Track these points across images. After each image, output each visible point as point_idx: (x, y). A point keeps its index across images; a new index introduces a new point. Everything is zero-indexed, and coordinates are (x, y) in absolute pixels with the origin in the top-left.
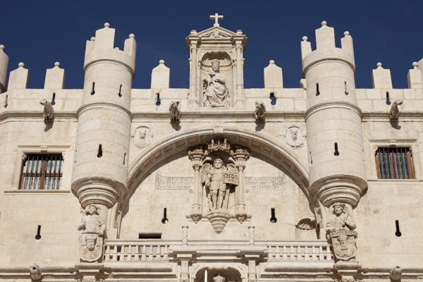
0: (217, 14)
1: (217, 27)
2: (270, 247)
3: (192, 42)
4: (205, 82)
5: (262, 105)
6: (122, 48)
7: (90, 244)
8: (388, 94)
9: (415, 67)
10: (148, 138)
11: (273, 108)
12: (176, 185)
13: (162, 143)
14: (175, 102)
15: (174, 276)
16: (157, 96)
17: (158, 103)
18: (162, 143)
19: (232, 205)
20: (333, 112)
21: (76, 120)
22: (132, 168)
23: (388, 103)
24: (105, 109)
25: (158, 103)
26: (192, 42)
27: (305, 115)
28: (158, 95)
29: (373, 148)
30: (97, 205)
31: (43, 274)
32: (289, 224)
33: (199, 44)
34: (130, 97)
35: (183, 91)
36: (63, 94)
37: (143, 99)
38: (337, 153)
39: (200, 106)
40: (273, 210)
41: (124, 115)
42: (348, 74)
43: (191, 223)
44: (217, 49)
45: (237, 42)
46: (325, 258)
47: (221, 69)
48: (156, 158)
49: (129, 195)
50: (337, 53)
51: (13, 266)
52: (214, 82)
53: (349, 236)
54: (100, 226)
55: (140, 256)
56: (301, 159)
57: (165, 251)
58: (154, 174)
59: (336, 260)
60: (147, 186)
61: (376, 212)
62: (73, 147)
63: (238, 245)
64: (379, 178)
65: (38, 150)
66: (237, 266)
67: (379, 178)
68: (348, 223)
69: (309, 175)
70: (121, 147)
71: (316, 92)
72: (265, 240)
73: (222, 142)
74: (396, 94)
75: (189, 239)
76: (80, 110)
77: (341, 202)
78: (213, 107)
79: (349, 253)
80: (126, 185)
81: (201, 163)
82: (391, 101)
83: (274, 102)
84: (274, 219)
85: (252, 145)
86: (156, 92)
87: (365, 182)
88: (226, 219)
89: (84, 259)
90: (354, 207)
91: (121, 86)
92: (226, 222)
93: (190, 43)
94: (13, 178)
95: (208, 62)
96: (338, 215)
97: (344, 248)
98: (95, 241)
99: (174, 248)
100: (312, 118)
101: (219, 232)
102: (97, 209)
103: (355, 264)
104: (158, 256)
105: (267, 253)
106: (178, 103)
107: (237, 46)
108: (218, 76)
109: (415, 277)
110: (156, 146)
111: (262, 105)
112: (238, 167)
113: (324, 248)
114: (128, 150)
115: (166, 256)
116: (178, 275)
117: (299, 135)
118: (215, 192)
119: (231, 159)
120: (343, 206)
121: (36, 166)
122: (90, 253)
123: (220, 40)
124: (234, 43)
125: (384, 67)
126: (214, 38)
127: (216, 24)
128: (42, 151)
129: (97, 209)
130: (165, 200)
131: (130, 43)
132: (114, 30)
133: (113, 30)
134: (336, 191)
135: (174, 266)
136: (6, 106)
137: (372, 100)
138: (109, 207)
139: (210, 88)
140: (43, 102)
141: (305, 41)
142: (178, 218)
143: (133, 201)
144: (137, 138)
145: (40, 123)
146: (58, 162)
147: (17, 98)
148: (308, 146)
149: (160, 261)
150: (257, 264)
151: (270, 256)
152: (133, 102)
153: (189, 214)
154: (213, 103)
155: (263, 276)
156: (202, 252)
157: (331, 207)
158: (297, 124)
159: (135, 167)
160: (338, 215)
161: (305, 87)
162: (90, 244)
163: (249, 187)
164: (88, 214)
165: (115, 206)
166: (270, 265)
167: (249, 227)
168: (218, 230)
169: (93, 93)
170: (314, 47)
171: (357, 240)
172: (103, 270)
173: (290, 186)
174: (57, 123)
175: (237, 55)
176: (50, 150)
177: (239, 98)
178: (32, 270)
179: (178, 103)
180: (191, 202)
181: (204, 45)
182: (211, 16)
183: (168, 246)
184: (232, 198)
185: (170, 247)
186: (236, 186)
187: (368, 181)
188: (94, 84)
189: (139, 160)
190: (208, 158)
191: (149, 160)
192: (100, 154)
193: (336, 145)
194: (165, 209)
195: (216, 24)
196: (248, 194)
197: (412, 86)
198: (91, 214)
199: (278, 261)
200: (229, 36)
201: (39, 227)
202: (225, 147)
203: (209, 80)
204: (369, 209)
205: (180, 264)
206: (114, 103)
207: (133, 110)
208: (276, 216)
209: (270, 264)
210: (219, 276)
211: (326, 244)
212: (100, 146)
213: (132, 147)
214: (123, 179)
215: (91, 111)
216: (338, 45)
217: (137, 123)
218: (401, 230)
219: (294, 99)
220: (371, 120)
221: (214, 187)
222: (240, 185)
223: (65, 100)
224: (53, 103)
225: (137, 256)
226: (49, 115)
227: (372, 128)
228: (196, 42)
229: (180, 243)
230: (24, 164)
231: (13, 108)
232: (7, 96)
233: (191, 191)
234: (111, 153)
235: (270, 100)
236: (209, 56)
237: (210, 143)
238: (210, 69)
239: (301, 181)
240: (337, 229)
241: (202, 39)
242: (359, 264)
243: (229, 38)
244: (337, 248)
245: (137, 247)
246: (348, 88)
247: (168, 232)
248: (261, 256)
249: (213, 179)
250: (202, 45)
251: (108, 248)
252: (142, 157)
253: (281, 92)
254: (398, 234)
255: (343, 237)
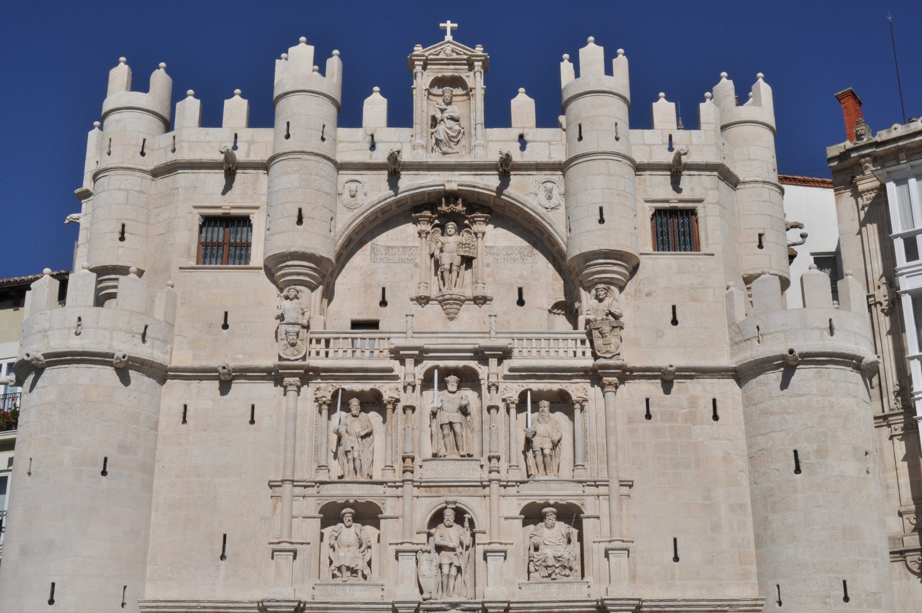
0: (449, 22)
1: (449, 42)
2: (516, 340)
3: (416, 63)
4: (434, 119)
5: (507, 155)
6: (322, 71)
7: (291, 337)
8: (670, 137)
9: (708, 100)
10: (360, 196)
11: (522, 156)
12: (397, 256)
13: (379, 202)
14: (395, 150)
15: (396, 378)
16: (370, 138)
17: (373, 147)
18: (379, 202)
19: (465, 284)
20: (598, 165)
21: (266, 172)
22: (341, 236)
23: (671, 149)
24: (305, 160)
25: (373, 147)
26: (416, 63)
27: (562, 167)
28: (372, 136)
29: (648, 211)
30: (299, 288)
31: (233, 374)
32: (539, 308)
33: (424, 68)
34: (335, 140)
35: (405, 132)
36: (247, 134)
37: (352, 142)
38: (602, 221)
39: (427, 151)
40: (520, 290)
41: (329, 167)
42: (620, 112)
43: (415, 308)
44: (449, 71)
45: (476, 63)
46: (584, 353)
47: (454, 99)
48: (371, 222)
49: (336, 272)
50: (608, 83)
51: (197, 364)
52: (445, 120)
53: (614, 327)
54: (303, 314)
55: (354, 352)
56: (556, 224)
57: (386, 345)
58: (368, 246)
59: (596, 357)
60: (360, 258)
61: (648, 294)
62: (264, 207)
63: (475, 338)
64: (654, 250)
65: (219, 212)
66: (473, 364)
67: (654, 250)
68: (612, 311)
69: (567, 247)
70: (326, 210)
71: (578, 136)
72: (510, 331)
73: (457, 199)
74: (682, 138)
75: (415, 331)
76: (272, 159)
77: (605, 283)
78: (444, 153)
79: (612, 348)
80: (334, 261)
81: (428, 228)
82: (674, 146)
83: (523, 148)
84: (521, 302)
85: (495, 204)
86: (370, 133)
87: (637, 257)
88: (461, 301)
89: (285, 357)
90: (621, 289)
91: (324, 126)
92: (461, 306)
93: (413, 66)
94: (189, 249)
95: (436, 91)
96: (601, 301)
97: (606, 343)
98: (298, 334)
99: (398, 342)
100: (572, 171)
101: (452, 319)
102: (298, 292)
103: (619, 362)
104: (376, 353)
105: (512, 348)
106: (399, 152)
107: (476, 69)
108: (453, 110)
109: (691, 377)
110: (371, 208)
111: (507, 155)
112: (476, 234)
113: (583, 342)
114: (335, 213)
115: (386, 353)
116: (402, 376)
117: (555, 193)
118: (447, 267)
119: (466, 222)
120: (608, 290)
121: (218, 234)
122: (292, 349)
123: (453, 60)
124: (471, 66)
125: (668, 98)
126: (445, 57)
127: (449, 37)
128: (223, 213)
129: (298, 292)
130: (382, 278)
131: (334, 63)
132: (313, 47)
133: (311, 49)
134: (599, 269)
135: (395, 364)
136: (174, 151)
137: (649, 145)
138: (313, 288)
139: (441, 128)
140: (223, 150)
141: (566, 61)
142: (400, 301)
143: (342, 283)
144: (346, 196)
145: (219, 177)
146: (245, 229)
147: (187, 141)
148: (566, 208)
149: (378, 358)
150: (500, 363)
151: (515, 353)
152: (340, 146)
153: (414, 295)
154: (444, 149)
155: (506, 377)
156: (431, 347)
157: (593, 292)
158: (553, 178)
159: (344, 236)
160: (601, 301)
161: (564, 126)
162: (292, 338)
163: (490, 259)
164: (287, 298)
165: (321, 287)
166: (515, 362)
167: (490, 316)
168: (451, 316)
169: (288, 136)
170: (577, 75)
171: (623, 333)
172: (308, 369)
173: (541, 262)
174: (240, 176)
175: (476, 81)
176: (234, 212)
177: (478, 142)
178: (220, 369)
179: (399, 152)
180: (417, 279)
181: (432, 67)
182: (441, 25)
183: (389, 339)
184: (467, 274)
185: (392, 341)
186: (473, 258)
187: (641, 254)
188: (288, 124)
189: (350, 225)
190: (437, 222)
191: (362, 225)
192: (300, 221)
193: (601, 209)
194: (384, 289)
195: (449, 37)
196: (489, 269)
197: (703, 126)
198: (291, 300)
199: (525, 358)
200: (465, 54)
201: (226, 314)
202: (460, 208)
203: (439, 116)
204: (640, 290)
205: (403, 363)
206: (316, 151)
207: (340, 158)
208: (525, 298)
209: (515, 362)
210: (452, 376)
211: (584, 336)
212: (300, 210)
213: (340, 205)
214: (328, 252)
215: (285, 162)
216: (609, 71)
217: (346, 176)
218: (678, 318)
219: (549, 143)
220: (648, 172)
221: (446, 260)
222: (479, 257)
223: (251, 143)
224: (235, 147)
225: (350, 352)
226: (231, 166)
227: (648, 184)
228: (422, 63)
229: (404, 335)
230: (201, 232)
231: (185, 154)
232: (174, 137)
233: (416, 265)
234: (313, 219)
235: (519, 144)
236: (439, 82)
237: (441, 205)
238: (440, 100)
239: (554, 254)
240: (599, 318)
241: (431, 57)
242: (624, 363)
243: (465, 57)
244: (598, 342)
245: (350, 340)
246: (619, 131)
247: (388, 319)
248: (504, 352)
249: (444, 249)
250: (429, 67)
251: (314, 341)
252: (353, 222)
253: (534, 134)
254: (675, 322)
255: (606, 328)
